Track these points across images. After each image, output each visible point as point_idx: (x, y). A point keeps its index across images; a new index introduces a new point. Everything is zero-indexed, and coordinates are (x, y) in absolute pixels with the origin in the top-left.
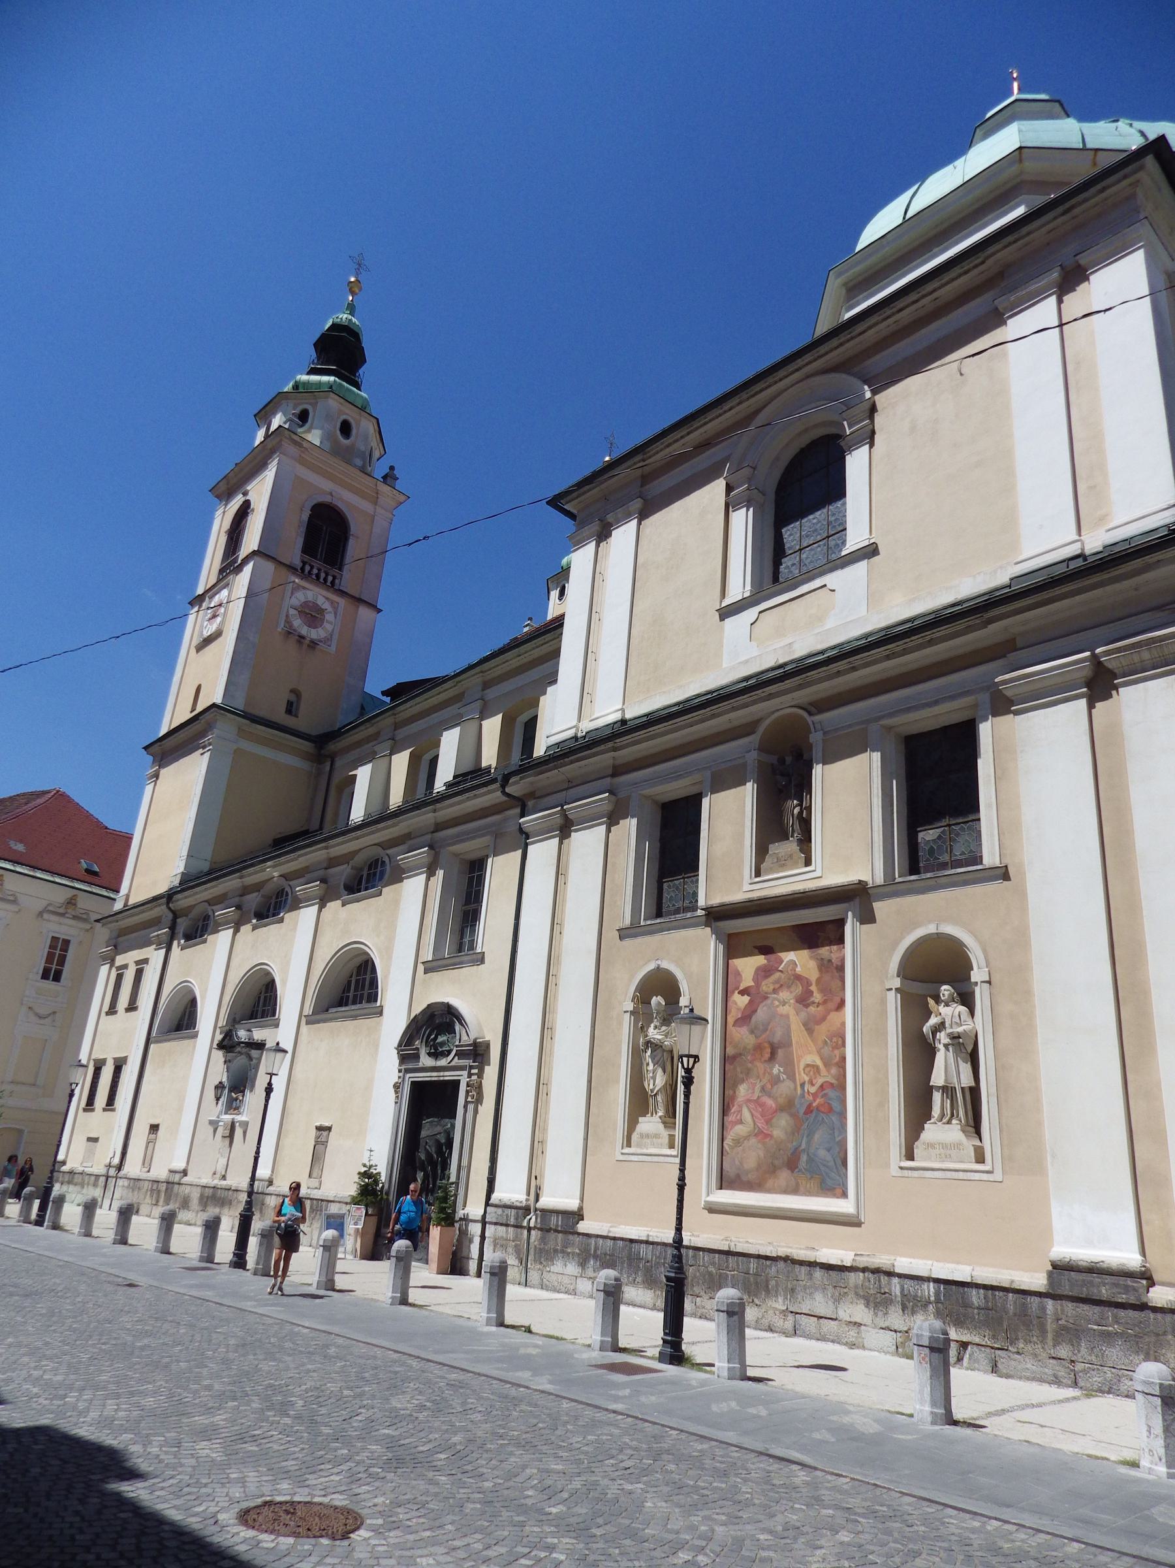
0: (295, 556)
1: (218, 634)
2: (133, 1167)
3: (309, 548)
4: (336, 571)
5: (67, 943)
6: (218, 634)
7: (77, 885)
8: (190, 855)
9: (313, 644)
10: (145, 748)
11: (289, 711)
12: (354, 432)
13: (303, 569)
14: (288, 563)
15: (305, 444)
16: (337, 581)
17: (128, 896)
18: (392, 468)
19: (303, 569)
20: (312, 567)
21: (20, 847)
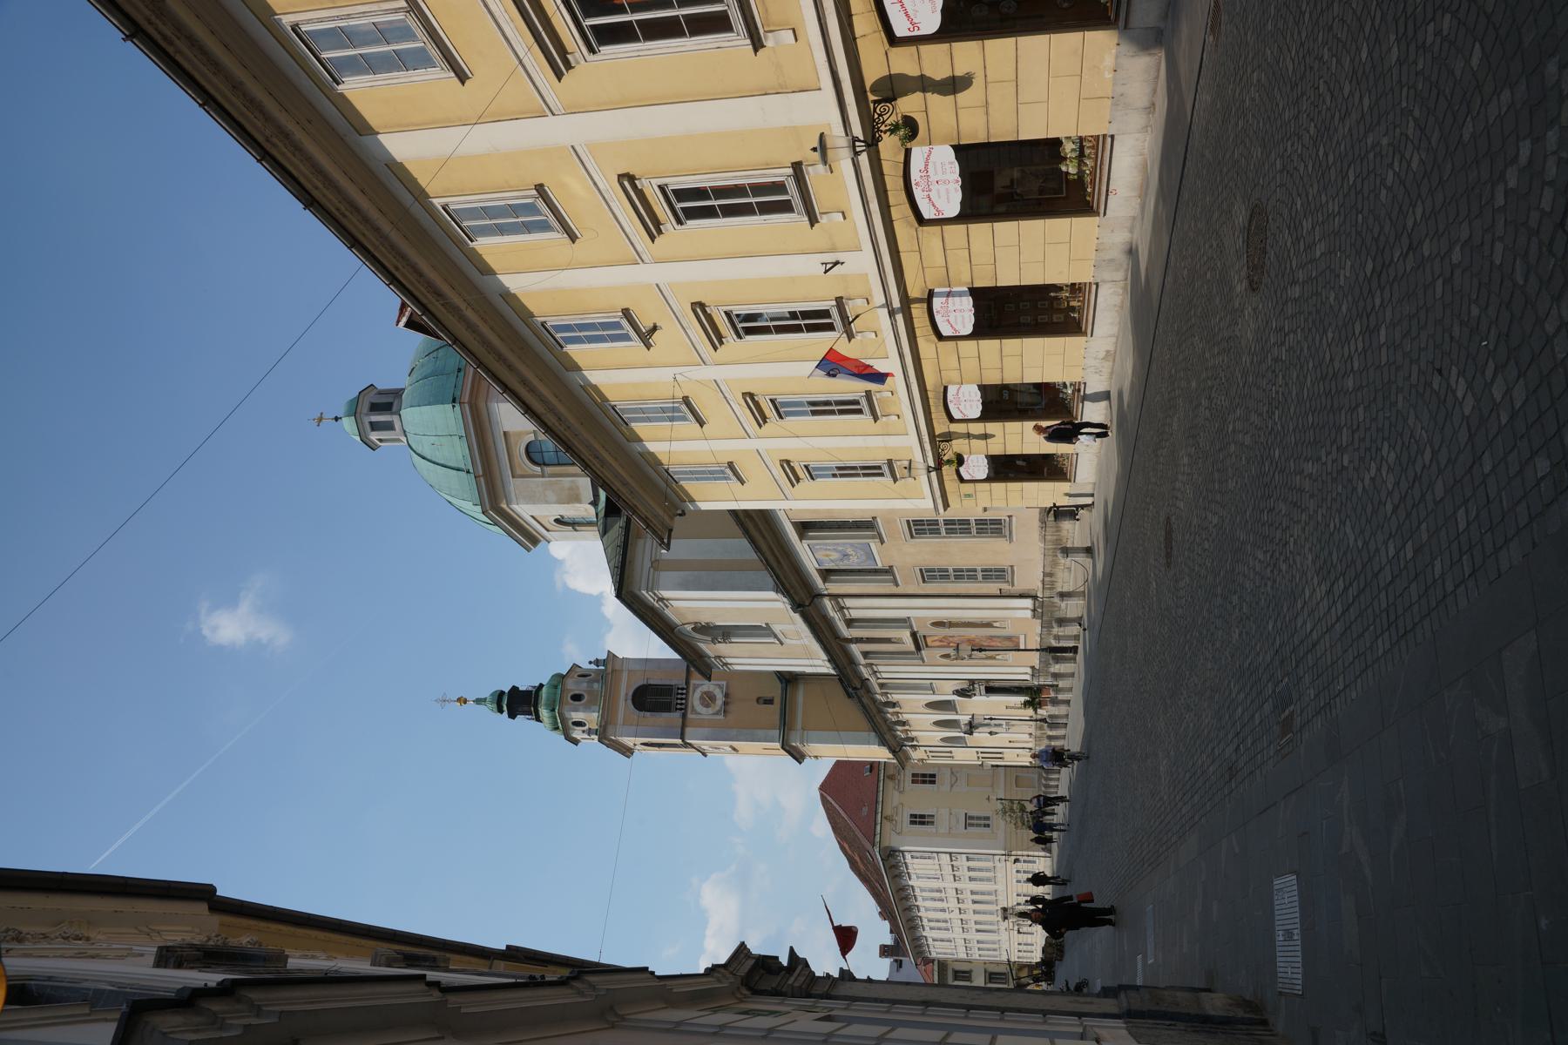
0: (676, 716)
1: (731, 747)
2: (1030, 745)
3: (667, 708)
4: (675, 691)
5: (914, 775)
6: (731, 747)
7: (882, 778)
8: (869, 744)
9: (727, 695)
10: (800, 763)
11: (770, 701)
12: (577, 692)
13: (681, 709)
14: (681, 720)
15: (603, 724)
16: (680, 687)
17: (889, 759)
18: (590, 663)
19: (681, 709)
20: (677, 704)
21: (865, 810)
